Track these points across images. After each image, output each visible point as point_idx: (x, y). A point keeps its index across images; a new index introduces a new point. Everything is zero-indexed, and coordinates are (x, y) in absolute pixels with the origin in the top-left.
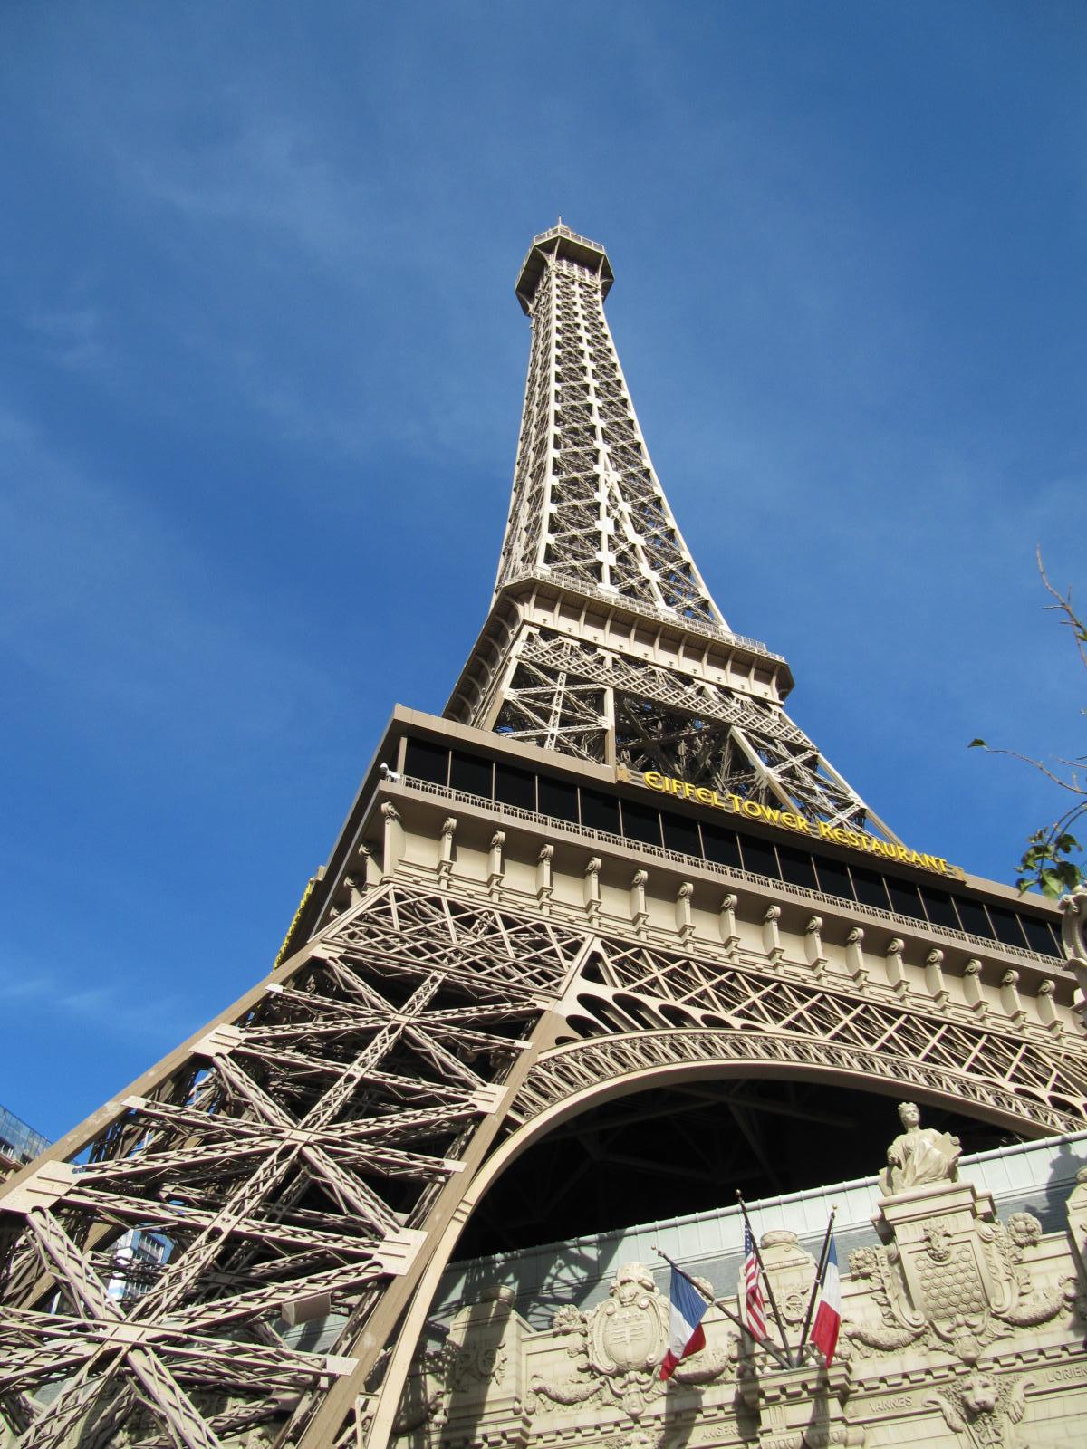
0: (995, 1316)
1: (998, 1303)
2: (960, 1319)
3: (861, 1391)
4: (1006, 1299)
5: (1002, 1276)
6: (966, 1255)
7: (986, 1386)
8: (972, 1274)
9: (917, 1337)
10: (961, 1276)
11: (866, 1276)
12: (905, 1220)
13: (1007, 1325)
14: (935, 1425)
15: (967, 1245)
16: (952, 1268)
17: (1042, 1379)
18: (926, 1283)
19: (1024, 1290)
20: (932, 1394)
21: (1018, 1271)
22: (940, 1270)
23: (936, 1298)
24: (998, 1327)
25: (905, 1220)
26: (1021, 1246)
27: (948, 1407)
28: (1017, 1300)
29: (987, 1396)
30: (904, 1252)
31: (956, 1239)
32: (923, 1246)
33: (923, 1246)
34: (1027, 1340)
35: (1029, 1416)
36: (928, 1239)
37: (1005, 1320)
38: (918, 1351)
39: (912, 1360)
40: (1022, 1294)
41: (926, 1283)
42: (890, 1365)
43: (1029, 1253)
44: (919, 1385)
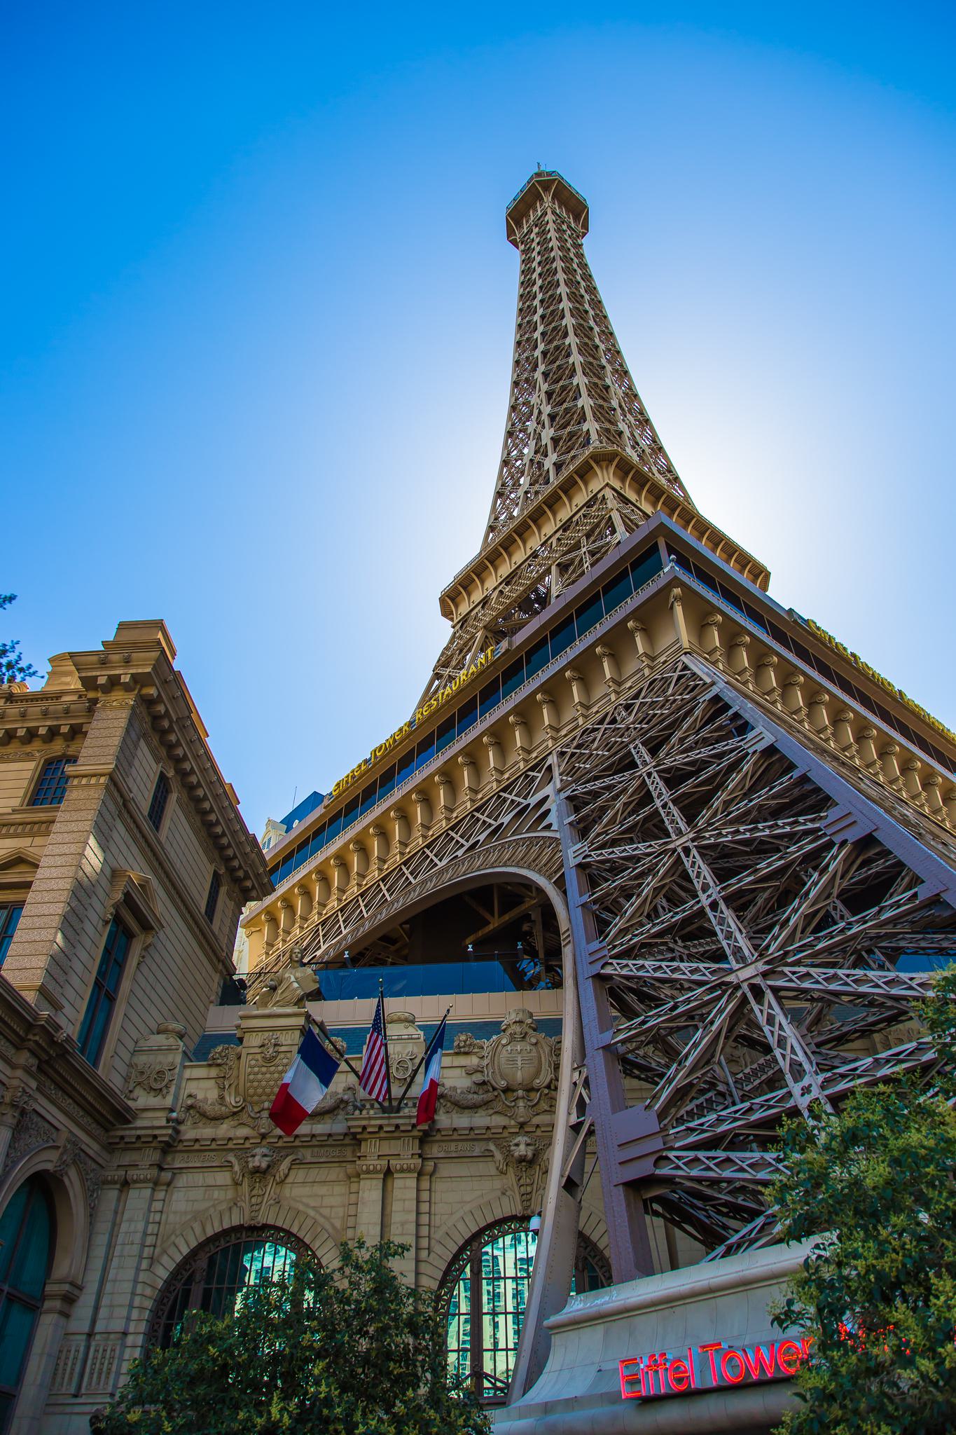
3: (180, 1147)
7: (265, 1155)
9: (235, 1114)
14: (223, 1178)
15: (288, 1055)
16: (272, 1069)
17: (307, 1155)
18: (252, 1077)
27: (237, 1168)
31: (283, 1049)
36: (263, 1046)
42: (207, 1132)
44: (223, 1149)
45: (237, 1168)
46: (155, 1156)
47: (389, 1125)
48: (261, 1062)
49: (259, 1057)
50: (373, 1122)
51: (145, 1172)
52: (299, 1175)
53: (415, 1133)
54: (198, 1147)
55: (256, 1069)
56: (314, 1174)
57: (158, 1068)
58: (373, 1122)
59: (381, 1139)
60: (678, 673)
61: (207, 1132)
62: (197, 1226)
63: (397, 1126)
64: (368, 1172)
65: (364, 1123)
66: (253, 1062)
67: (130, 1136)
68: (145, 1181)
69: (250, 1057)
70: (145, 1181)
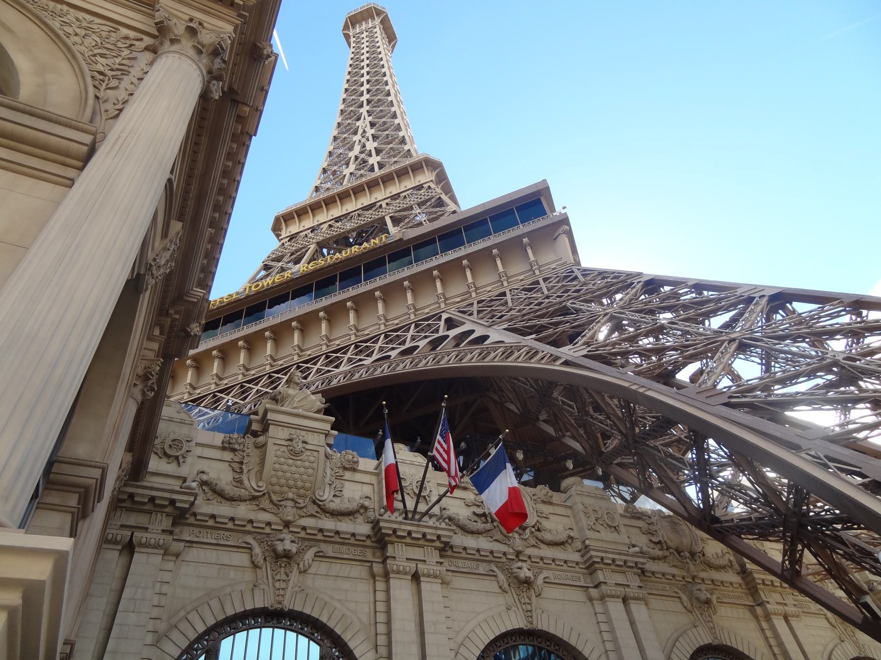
0: (314, 502)
1: (321, 493)
2: (291, 495)
4: (326, 495)
5: (327, 480)
6: (312, 459)
8: (310, 471)
9: (254, 498)
10: (302, 470)
11: (234, 450)
12: (279, 424)
13: (319, 510)
15: (315, 454)
16: (299, 463)
17: (329, 549)
18: (277, 466)
19: (337, 493)
20: (249, 539)
21: (337, 483)
22: (290, 462)
23: (279, 478)
24: (313, 509)
25: (279, 424)
26: (345, 469)
28: (331, 497)
29: (294, 548)
30: (270, 442)
32: (286, 443)
33: (286, 443)
34: (328, 524)
35: (312, 570)
36: (291, 440)
37: (319, 506)
38: (250, 506)
39: (243, 511)
40: (335, 496)
41: (277, 466)
42: (224, 510)
43: (348, 475)
45: (257, 550)
46: (166, 523)
47: (417, 532)
48: (287, 454)
49: (285, 449)
50: (403, 527)
51: (157, 537)
52: (322, 567)
53: (437, 544)
54: (215, 523)
55: (282, 460)
56: (337, 568)
57: (172, 437)
58: (403, 527)
59: (407, 545)
60: (316, 367)
61: (224, 510)
62: (215, 604)
63: (424, 535)
64: (398, 572)
65: (395, 526)
66: (279, 453)
67: (143, 495)
68: (157, 546)
69: (276, 447)
70: (157, 546)
